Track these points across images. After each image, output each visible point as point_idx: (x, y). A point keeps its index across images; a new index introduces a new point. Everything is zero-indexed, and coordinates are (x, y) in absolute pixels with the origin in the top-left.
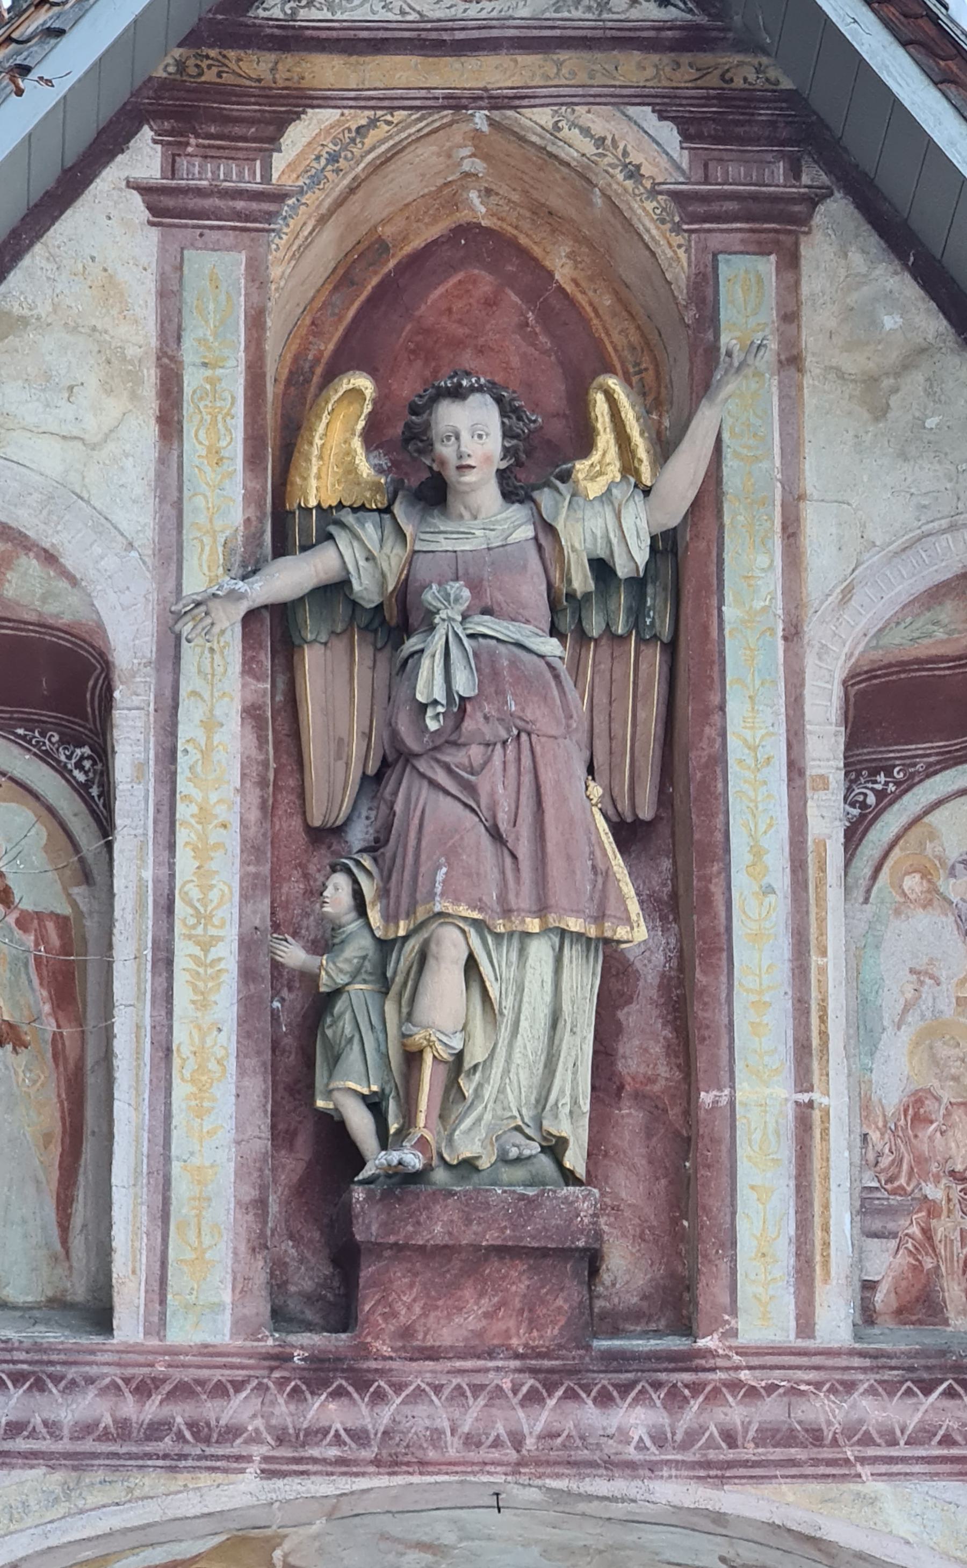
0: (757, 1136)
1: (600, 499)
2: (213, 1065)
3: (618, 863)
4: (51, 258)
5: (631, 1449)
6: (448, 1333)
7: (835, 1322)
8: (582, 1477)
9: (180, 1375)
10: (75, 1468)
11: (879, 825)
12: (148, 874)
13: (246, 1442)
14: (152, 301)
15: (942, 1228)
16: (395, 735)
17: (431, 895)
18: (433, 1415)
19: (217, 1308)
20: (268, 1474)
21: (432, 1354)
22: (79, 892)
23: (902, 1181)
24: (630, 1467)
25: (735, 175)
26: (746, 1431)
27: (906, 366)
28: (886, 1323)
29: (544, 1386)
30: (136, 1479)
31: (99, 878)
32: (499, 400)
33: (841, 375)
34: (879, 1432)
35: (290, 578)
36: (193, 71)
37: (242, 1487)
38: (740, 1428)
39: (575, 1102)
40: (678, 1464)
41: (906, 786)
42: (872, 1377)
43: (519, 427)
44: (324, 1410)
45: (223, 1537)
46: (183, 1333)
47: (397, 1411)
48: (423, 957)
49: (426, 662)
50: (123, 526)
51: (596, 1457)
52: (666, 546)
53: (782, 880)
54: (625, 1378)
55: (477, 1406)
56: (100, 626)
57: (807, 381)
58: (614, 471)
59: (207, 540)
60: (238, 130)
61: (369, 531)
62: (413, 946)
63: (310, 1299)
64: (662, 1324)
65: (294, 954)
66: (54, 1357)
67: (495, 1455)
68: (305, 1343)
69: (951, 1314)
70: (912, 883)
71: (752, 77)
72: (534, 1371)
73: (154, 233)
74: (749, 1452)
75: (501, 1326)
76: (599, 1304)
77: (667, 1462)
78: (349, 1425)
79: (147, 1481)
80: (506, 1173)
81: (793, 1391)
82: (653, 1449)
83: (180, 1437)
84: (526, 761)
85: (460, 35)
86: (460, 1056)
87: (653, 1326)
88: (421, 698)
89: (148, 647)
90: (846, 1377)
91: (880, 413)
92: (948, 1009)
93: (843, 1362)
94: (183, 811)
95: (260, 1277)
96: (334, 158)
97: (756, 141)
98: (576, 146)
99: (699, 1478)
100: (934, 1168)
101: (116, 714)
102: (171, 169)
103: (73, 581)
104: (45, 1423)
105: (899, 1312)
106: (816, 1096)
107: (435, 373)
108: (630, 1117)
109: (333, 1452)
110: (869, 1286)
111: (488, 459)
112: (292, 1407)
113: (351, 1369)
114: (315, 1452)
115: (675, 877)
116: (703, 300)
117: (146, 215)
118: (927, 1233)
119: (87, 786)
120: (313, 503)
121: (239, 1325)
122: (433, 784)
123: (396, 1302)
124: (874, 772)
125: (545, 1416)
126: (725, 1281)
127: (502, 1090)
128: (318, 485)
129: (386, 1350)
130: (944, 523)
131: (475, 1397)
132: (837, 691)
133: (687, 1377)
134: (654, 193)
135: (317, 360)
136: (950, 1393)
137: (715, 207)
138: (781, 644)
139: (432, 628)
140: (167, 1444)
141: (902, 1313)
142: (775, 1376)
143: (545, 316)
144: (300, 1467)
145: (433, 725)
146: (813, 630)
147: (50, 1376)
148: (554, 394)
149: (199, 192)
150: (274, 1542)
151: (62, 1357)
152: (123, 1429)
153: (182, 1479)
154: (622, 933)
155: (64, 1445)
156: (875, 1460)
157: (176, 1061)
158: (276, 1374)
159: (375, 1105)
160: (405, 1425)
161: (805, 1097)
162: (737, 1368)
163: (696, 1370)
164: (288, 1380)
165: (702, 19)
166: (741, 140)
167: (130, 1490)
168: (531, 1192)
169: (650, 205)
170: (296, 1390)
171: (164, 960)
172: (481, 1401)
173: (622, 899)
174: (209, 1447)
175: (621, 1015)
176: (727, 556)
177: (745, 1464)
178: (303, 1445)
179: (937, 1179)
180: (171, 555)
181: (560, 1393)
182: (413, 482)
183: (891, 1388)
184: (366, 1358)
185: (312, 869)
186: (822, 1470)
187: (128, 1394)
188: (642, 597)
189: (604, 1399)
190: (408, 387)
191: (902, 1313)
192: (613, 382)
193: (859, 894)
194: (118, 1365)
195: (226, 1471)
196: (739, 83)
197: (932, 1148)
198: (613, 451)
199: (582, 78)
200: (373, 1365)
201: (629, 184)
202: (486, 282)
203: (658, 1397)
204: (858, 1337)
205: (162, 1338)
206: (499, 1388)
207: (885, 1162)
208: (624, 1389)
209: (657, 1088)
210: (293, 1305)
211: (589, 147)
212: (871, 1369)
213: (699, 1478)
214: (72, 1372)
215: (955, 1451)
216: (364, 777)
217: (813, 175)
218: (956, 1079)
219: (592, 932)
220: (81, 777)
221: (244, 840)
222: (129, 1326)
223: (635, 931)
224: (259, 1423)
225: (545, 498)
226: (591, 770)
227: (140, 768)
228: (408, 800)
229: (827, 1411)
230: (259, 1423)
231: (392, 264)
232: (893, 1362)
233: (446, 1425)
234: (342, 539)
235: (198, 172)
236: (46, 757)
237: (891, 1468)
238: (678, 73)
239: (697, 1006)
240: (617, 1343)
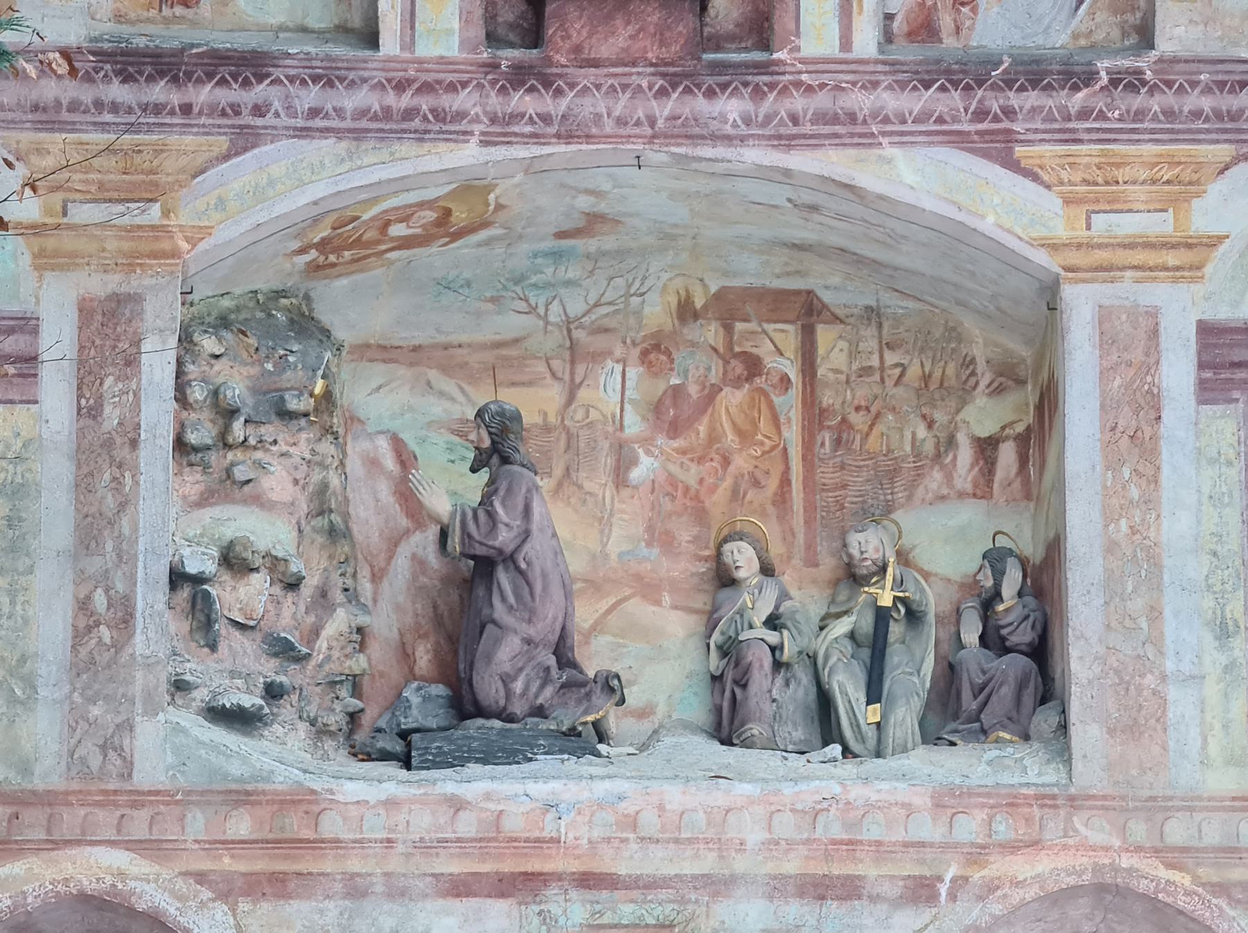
6: (605, 50)
7: (866, 41)
10: (356, 139)
13: (469, 122)
19: (449, 32)
21: (595, 63)
26: (805, 117)
28: (901, 42)
29: (670, 85)
30: (396, 146)
37: (467, 152)
38: (801, 113)
40: (759, 137)
44: (521, 101)
45: (455, 186)
47: (571, 101)
54: (725, 79)
55: (624, 98)
63: (512, 26)
64: (749, 44)
66: (340, 65)
67: (637, 131)
68: (509, 56)
69: (944, 35)
72: (664, 75)
74: (808, 129)
75: (641, 44)
76: (707, 30)
77: (752, 135)
78: (539, 111)
79: (403, 148)
81: (838, 88)
82: (743, 126)
83: (425, 118)
87: (743, 45)
90: (873, 78)
99: (773, 146)
104: (335, 109)
109: (528, 129)
110: (889, 17)
112: (500, 99)
113: (539, 74)
114: (516, 129)
126: (792, 14)
129: (563, 61)
133: (766, 78)
136: (942, 89)
140: (417, 123)
141: (911, 35)
142: (825, 78)
144: (507, 139)
147: (337, 77)
150: (489, 189)
151: (345, 65)
152: (387, 113)
153: (427, 146)
155: (348, 124)
156: (891, 134)
158: (490, 77)
160: (576, 111)
162: (800, 72)
163: (772, 74)
164: (497, 81)
167: (392, 154)
170: (503, 86)
172: (628, 95)
174: (445, 126)
177: (804, 136)
178: (508, 124)
181: (680, 89)
183: (903, 85)
184: (551, 66)
186: (856, 140)
187: (390, 90)
189: (710, 94)
191: (911, 35)
194: (383, 70)
195: (456, 141)
200: (555, 70)
203: (746, 92)
204: (881, 52)
205: (413, 52)
206: (640, 86)
208: (724, 87)
210: (501, 31)
213: (773, 146)
214: (351, 75)
215: (945, 127)
222: (390, 44)
224: (478, 109)
230: (478, 109)
232: (905, 68)
233: (604, 111)
237: (903, 139)
240: (719, 56)
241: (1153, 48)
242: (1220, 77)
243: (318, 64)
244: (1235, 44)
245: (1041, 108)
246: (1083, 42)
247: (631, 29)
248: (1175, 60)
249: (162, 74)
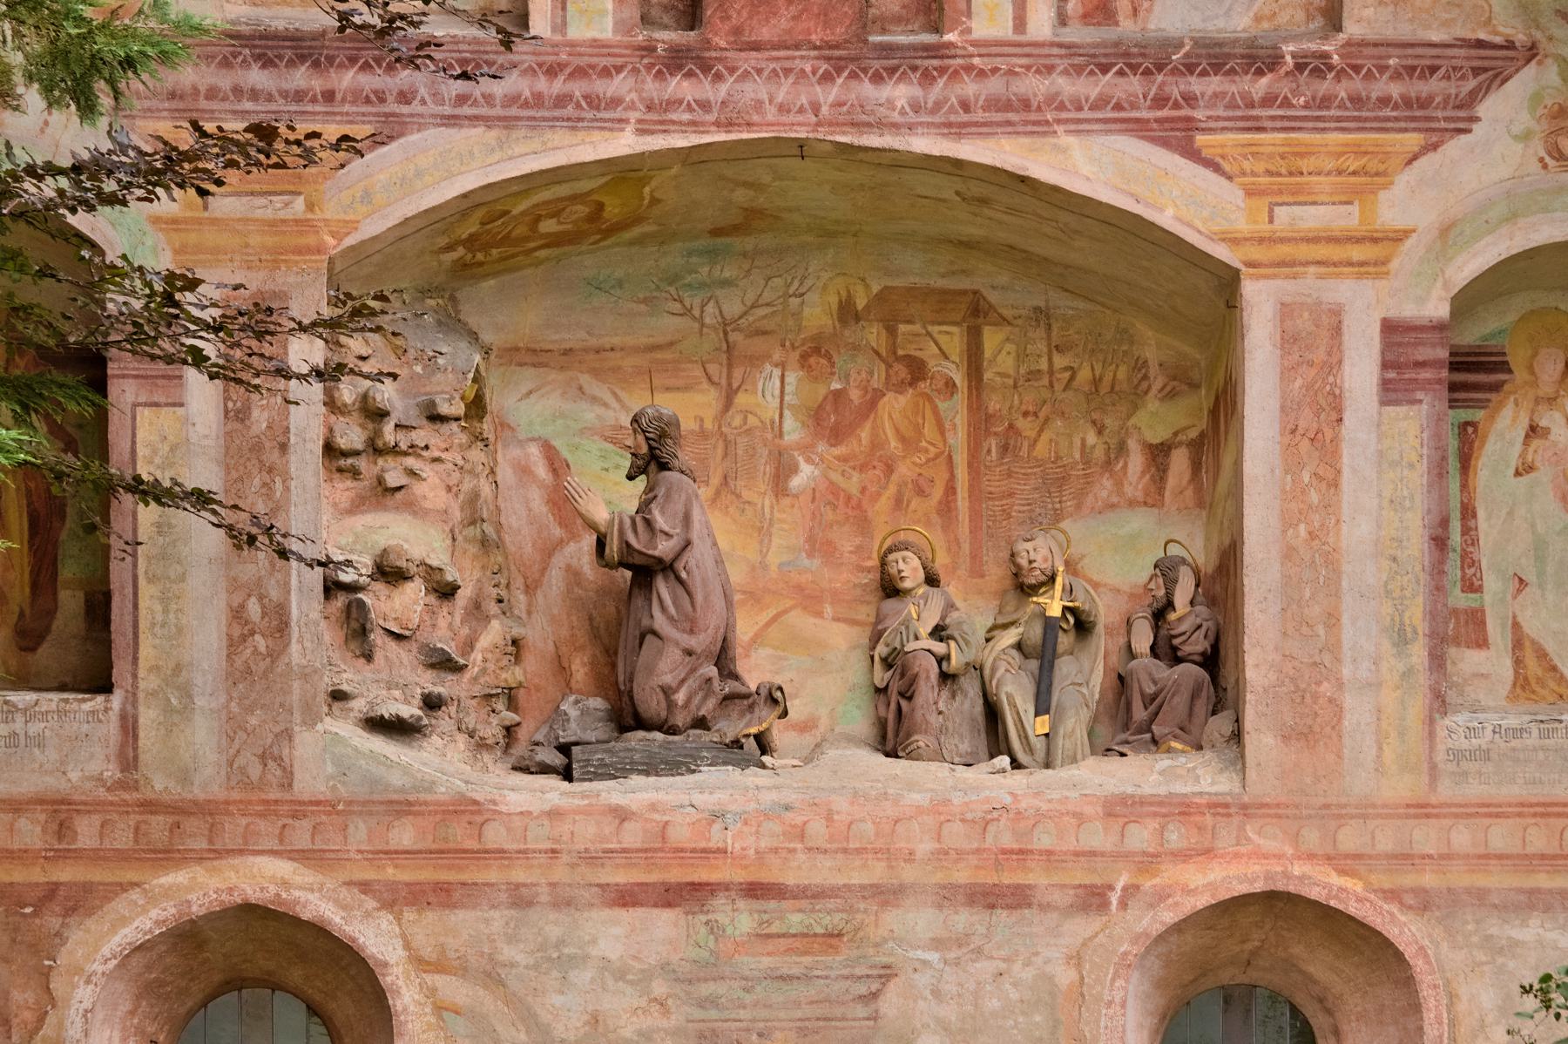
5: (896, 114)
6: (765, 33)
7: (1041, 24)
8: (862, 133)
9: (577, 61)
10: (506, 128)
19: (602, 13)
20: (641, 132)
21: (756, 47)
24: (895, 126)
26: (977, 101)
30: (549, 135)
34: (1071, 102)
37: (623, 141)
40: (929, 125)
42: (1067, 61)
44: (679, 87)
46: (577, 31)
51: (871, 119)
55: (787, 84)
63: (666, 8)
64: (916, 27)
67: (800, 118)
72: (828, 59)
74: (979, 116)
75: (802, 26)
77: (921, 124)
83: (578, 105)
87: (910, 27)
93: (1046, 51)
104: (483, 95)
105: (1085, 16)
109: (686, 117)
113: (698, 57)
114: (674, 116)
121: (619, 25)
125: (833, 93)
129: (723, 44)
131: (786, 77)
133: (936, 62)
136: (1121, 73)
140: (570, 110)
141: (1086, 18)
142: (998, 62)
144: (665, 127)
150: (644, 181)
152: (538, 100)
153: (581, 135)
156: (1067, 121)
158: (646, 61)
162: (972, 56)
163: (942, 57)
164: (653, 65)
167: (544, 143)
170: (659, 72)
172: (791, 80)
177: (976, 124)
181: (846, 74)
183: (1079, 69)
184: (709, 49)
186: (1030, 128)
189: (877, 79)
191: (1086, 18)
194: (534, 54)
195: (611, 130)
200: (714, 54)
206: (803, 71)
208: (892, 71)
210: (655, 13)
212: (1066, 56)
215: (1123, 115)
229: (1035, 86)
230: (634, 96)
232: (1081, 51)
233: (765, 97)
237: (1079, 127)
242: (1410, 62)
243: (466, 47)
244: (1429, 27)
245: (1224, 94)
246: (1265, 25)
247: (793, 10)
248: (1363, 44)
249: (302, 58)
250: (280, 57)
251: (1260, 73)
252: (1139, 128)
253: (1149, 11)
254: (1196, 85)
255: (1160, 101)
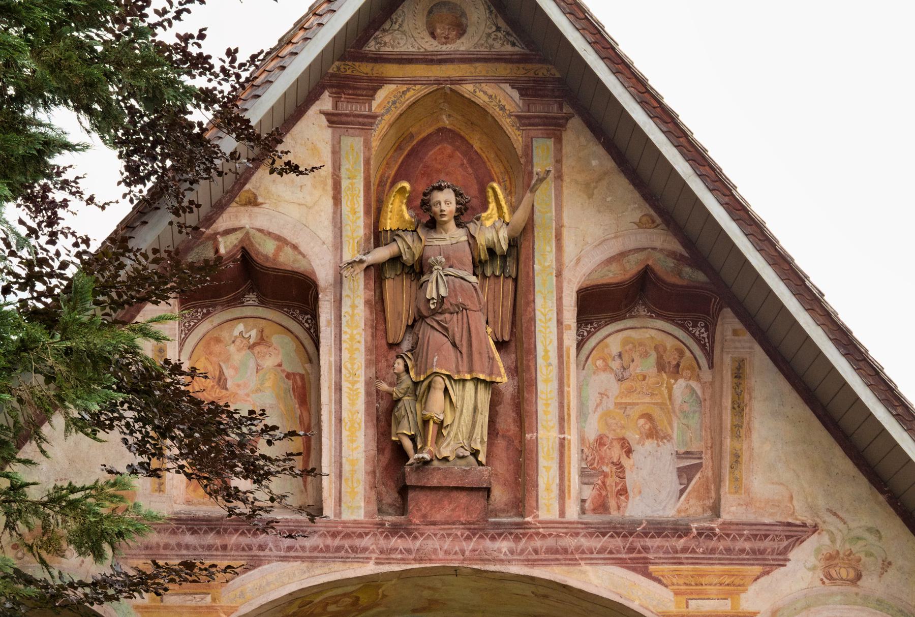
0: (546, 449)
1: (491, 227)
2: (356, 425)
3: (497, 355)
4: (293, 139)
7: (573, 513)
11: (588, 342)
12: (332, 359)
14: (330, 155)
15: (609, 481)
16: (419, 310)
17: (432, 366)
18: (433, 544)
19: (359, 508)
21: (434, 523)
22: (308, 366)
23: (595, 465)
25: (539, 109)
27: (600, 179)
31: (314, 359)
32: (454, 191)
33: (577, 182)
35: (382, 254)
36: (343, 70)
39: (482, 438)
41: (597, 329)
43: (462, 201)
44: (395, 542)
46: (346, 516)
48: (429, 387)
49: (430, 285)
50: (321, 236)
52: (513, 243)
53: (554, 361)
56: (314, 272)
57: (565, 184)
58: (495, 216)
59: (351, 241)
60: (359, 92)
61: (409, 239)
62: (426, 383)
63: (390, 505)
65: (384, 386)
68: (390, 519)
69: (612, 511)
70: (599, 363)
71: (545, 73)
72: (469, 529)
73: (330, 130)
74: (543, 556)
80: (459, 462)
84: (465, 320)
85: (439, 57)
86: (442, 422)
88: (428, 297)
89: (331, 279)
91: (590, 196)
92: (611, 406)
94: (344, 337)
95: (374, 498)
96: (394, 103)
97: (547, 96)
98: (481, 98)
100: (606, 461)
101: (320, 303)
102: (336, 106)
103: (304, 256)
106: (566, 436)
107: (431, 181)
108: (501, 443)
110: (583, 501)
111: (451, 212)
115: (516, 361)
116: (527, 155)
117: (327, 123)
118: (604, 483)
119: (309, 329)
120: (388, 228)
122: (432, 327)
123: (420, 503)
124: (587, 324)
126: (535, 499)
127: (457, 434)
128: (390, 223)
129: (418, 522)
130: (613, 235)
132: (574, 295)
133: (521, 531)
134: (510, 116)
135: (389, 177)
136: (612, 536)
137: (532, 121)
138: (554, 278)
139: (432, 272)
141: (595, 510)
143: (471, 161)
145: (432, 307)
146: (566, 274)
148: (474, 190)
149: (346, 115)
152: (327, 548)
154: (498, 379)
157: (343, 424)
159: (413, 438)
161: (562, 436)
165: (527, 51)
166: (542, 96)
168: (467, 469)
169: (508, 120)
170: (387, 535)
171: (339, 388)
172: (451, 539)
173: (498, 367)
174: (357, 554)
175: (497, 408)
176: (536, 247)
179: (607, 465)
180: (338, 246)
182: (424, 221)
183: (591, 535)
185: (389, 358)
188: (505, 262)
189: (493, 538)
190: (422, 188)
191: (595, 510)
192: (495, 185)
193: (581, 368)
196: (540, 75)
197: (606, 454)
198: (495, 209)
199: (484, 73)
200: (413, 527)
201: (501, 112)
202: (449, 149)
205: (340, 518)
207: (589, 459)
208: (500, 535)
209: (510, 433)
211: (487, 99)
216: (408, 326)
217: (567, 109)
218: (614, 430)
219: (488, 379)
220: (307, 326)
221: (366, 348)
223: (503, 379)
225: (471, 226)
226: (487, 323)
227: (329, 322)
228: (423, 334)
230: (374, 546)
231: (415, 142)
234: (399, 241)
235: (346, 108)
236: (295, 319)
238: (518, 71)
239: (525, 405)
240: (497, 520)
241: (719, 516)
242: (755, 532)
244: (763, 516)
245: (663, 547)
246: (683, 514)
247: (452, 506)
248: (731, 523)
249: (211, 530)
250: (200, 529)
251: (680, 537)
252: (621, 562)
253: (625, 507)
254: (649, 542)
255: (631, 550)
